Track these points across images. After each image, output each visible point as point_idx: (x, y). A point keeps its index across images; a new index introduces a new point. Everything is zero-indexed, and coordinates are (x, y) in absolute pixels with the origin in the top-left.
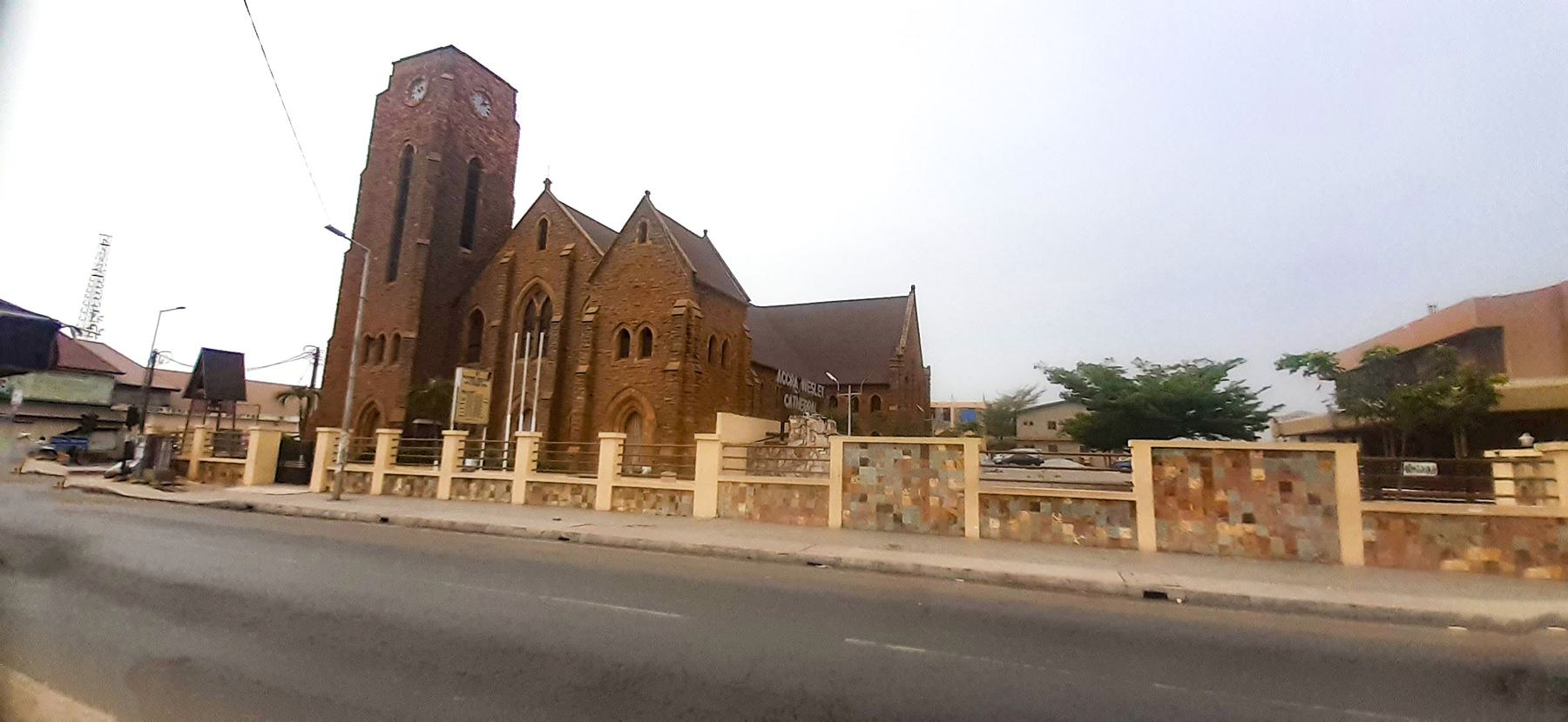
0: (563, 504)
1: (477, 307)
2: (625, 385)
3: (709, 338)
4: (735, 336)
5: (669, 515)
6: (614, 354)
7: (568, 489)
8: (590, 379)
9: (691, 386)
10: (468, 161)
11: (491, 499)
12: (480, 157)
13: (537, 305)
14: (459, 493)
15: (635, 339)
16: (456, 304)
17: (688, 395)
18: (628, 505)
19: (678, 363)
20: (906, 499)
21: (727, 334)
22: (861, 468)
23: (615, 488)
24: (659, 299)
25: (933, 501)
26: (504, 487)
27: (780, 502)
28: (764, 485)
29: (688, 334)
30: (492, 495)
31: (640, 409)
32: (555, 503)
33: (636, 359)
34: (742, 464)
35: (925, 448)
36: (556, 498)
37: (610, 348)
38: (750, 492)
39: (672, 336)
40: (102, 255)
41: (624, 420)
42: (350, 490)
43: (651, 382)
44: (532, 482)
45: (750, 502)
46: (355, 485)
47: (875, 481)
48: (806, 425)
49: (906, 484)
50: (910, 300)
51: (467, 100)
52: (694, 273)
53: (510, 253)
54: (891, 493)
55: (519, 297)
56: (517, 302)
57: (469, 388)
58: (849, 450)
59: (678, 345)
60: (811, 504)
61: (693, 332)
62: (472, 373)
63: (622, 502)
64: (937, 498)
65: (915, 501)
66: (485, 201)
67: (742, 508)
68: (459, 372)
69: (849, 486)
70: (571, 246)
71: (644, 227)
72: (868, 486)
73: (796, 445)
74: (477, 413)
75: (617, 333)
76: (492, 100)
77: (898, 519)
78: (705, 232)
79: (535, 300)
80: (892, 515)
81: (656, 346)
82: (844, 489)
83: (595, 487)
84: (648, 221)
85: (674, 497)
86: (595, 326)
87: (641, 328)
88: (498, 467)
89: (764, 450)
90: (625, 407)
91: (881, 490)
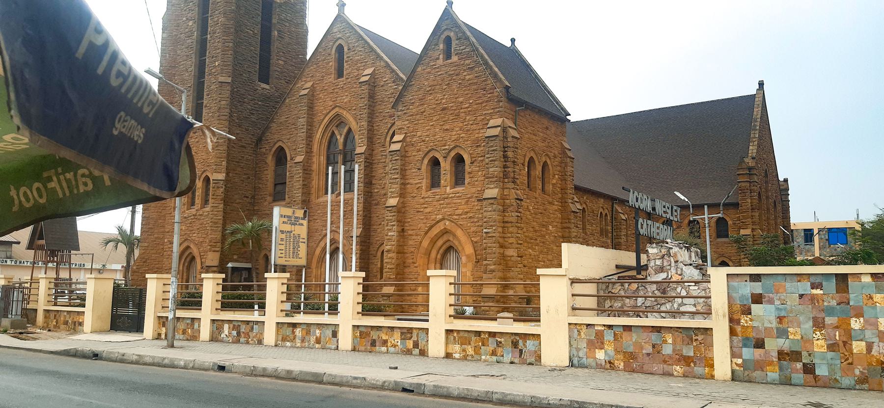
0: (392, 349)
1: (280, 144)
2: (440, 217)
3: (527, 160)
5: (512, 363)
6: (425, 183)
7: (397, 335)
8: (400, 211)
9: (512, 216)
11: (317, 346)
13: (338, 137)
14: (284, 339)
15: (446, 166)
16: (259, 141)
17: (509, 225)
18: (464, 350)
19: (496, 190)
20: (820, 345)
21: (547, 155)
22: (752, 305)
23: (449, 332)
24: (469, 120)
25: (858, 347)
26: (329, 333)
27: (648, 349)
28: (628, 328)
29: (505, 157)
30: (318, 341)
31: (456, 243)
32: (384, 349)
33: (448, 188)
34: (592, 303)
35: (842, 279)
36: (385, 343)
37: (420, 177)
38: (609, 336)
39: (487, 160)
41: (439, 256)
42: (181, 337)
43: (467, 213)
44: (358, 326)
45: (610, 348)
46: (184, 332)
47: (774, 324)
48: (670, 255)
49: (819, 324)
50: (758, 100)
52: (507, 88)
53: (309, 85)
54: (799, 337)
55: (320, 130)
56: (318, 135)
57: (287, 227)
58: (735, 284)
59: (495, 170)
60: (689, 352)
61: (510, 154)
62: (288, 211)
63: (457, 347)
64: (864, 344)
65: (832, 347)
66: (279, 31)
67: (600, 355)
68: (276, 211)
69: (739, 329)
70: (369, 71)
71: (448, 41)
72: (766, 329)
73: (659, 279)
74: (296, 254)
75: (426, 161)
77: (809, 369)
78: (513, 40)
79: (336, 132)
80: (799, 366)
81: (470, 173)
82: (732, 332)
83: (426, 330)
84: (452, 34)
85: (518, 342)
86: (403, 154)
87: (453, 154)
88: (316, 309)
89: (618, 287)
90: (440, 242)
91: (782, 333)
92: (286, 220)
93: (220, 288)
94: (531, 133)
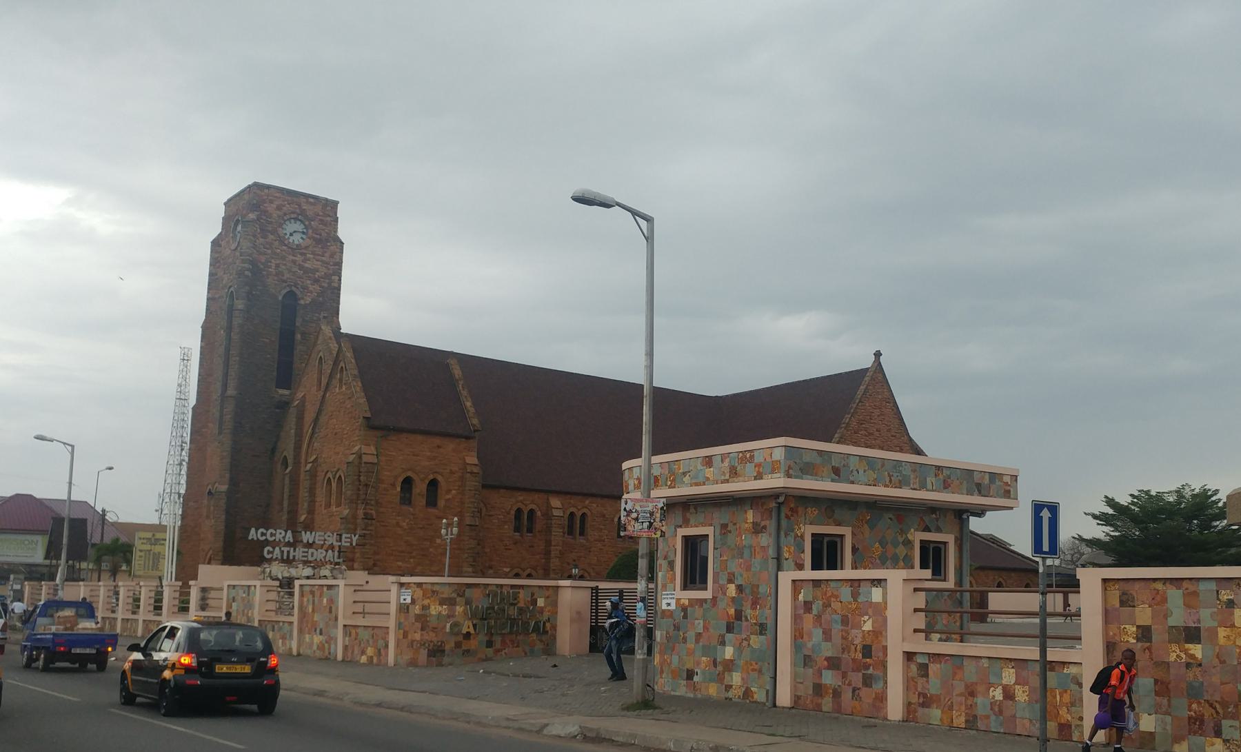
4: (452, 472)
10: (280, 298)
12: (294, 289)
16: (273, 450)
33: (334, 507)
40: (184, 373)
51: (274, 232)
57: (148, 547)
66: (303, 334)
76: (307, 223)
92: (145, 541)
93: (177, 595)
94: (408, 455)
